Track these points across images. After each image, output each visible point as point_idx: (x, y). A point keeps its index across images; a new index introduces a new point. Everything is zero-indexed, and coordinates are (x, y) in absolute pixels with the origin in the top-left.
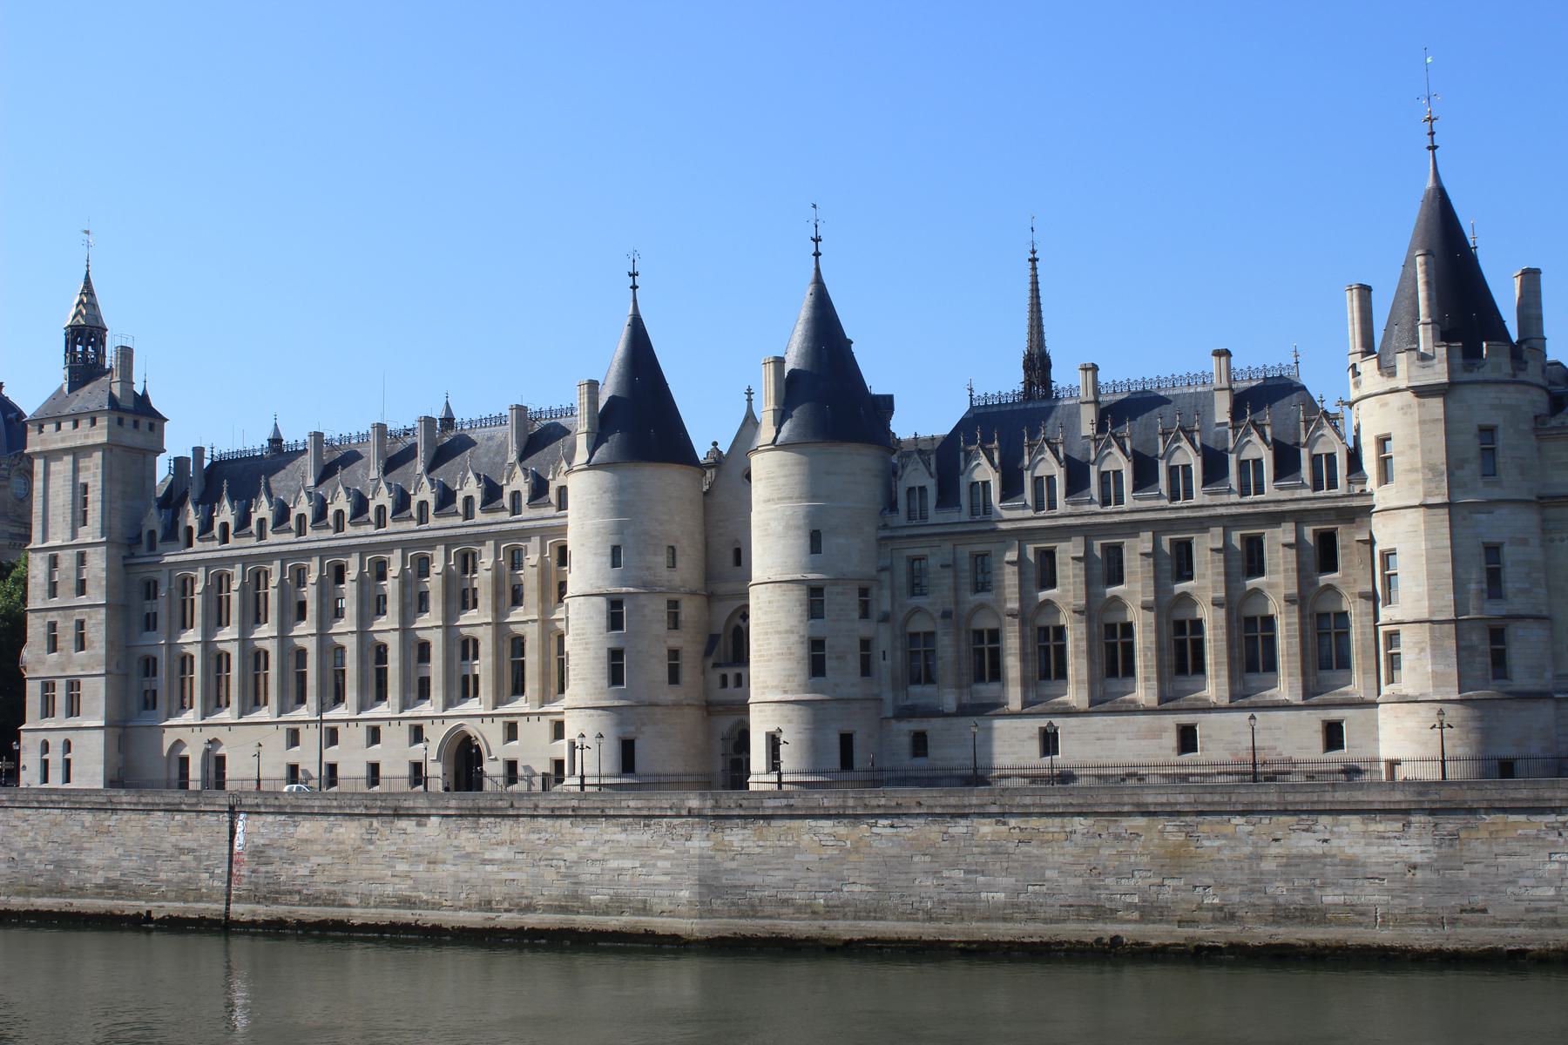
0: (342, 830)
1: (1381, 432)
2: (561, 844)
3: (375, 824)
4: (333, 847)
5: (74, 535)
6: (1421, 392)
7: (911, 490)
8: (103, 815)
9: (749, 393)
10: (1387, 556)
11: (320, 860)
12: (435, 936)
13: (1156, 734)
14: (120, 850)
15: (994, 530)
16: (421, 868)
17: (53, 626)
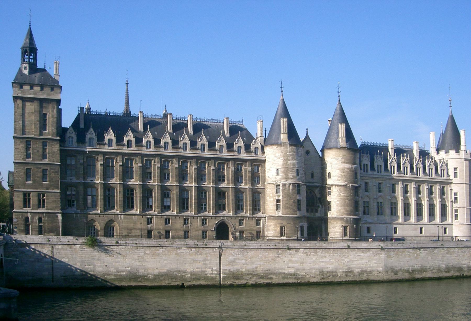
0: (267, 253)
1: (456, 167)
2: (344, 256)
3: (280, 251)
4: (263, 259)
5: (41, 134)
6: (466, 160)
7: (364, 164)
8: (154, 249)
9: (307, 129)
10: (456, 194)
11: (259, 263)
12: (309, 284)
13: (416, 229)
14: (166, 262)
15: (393, 179)
16: (298, 264)
17: (28, 170)
